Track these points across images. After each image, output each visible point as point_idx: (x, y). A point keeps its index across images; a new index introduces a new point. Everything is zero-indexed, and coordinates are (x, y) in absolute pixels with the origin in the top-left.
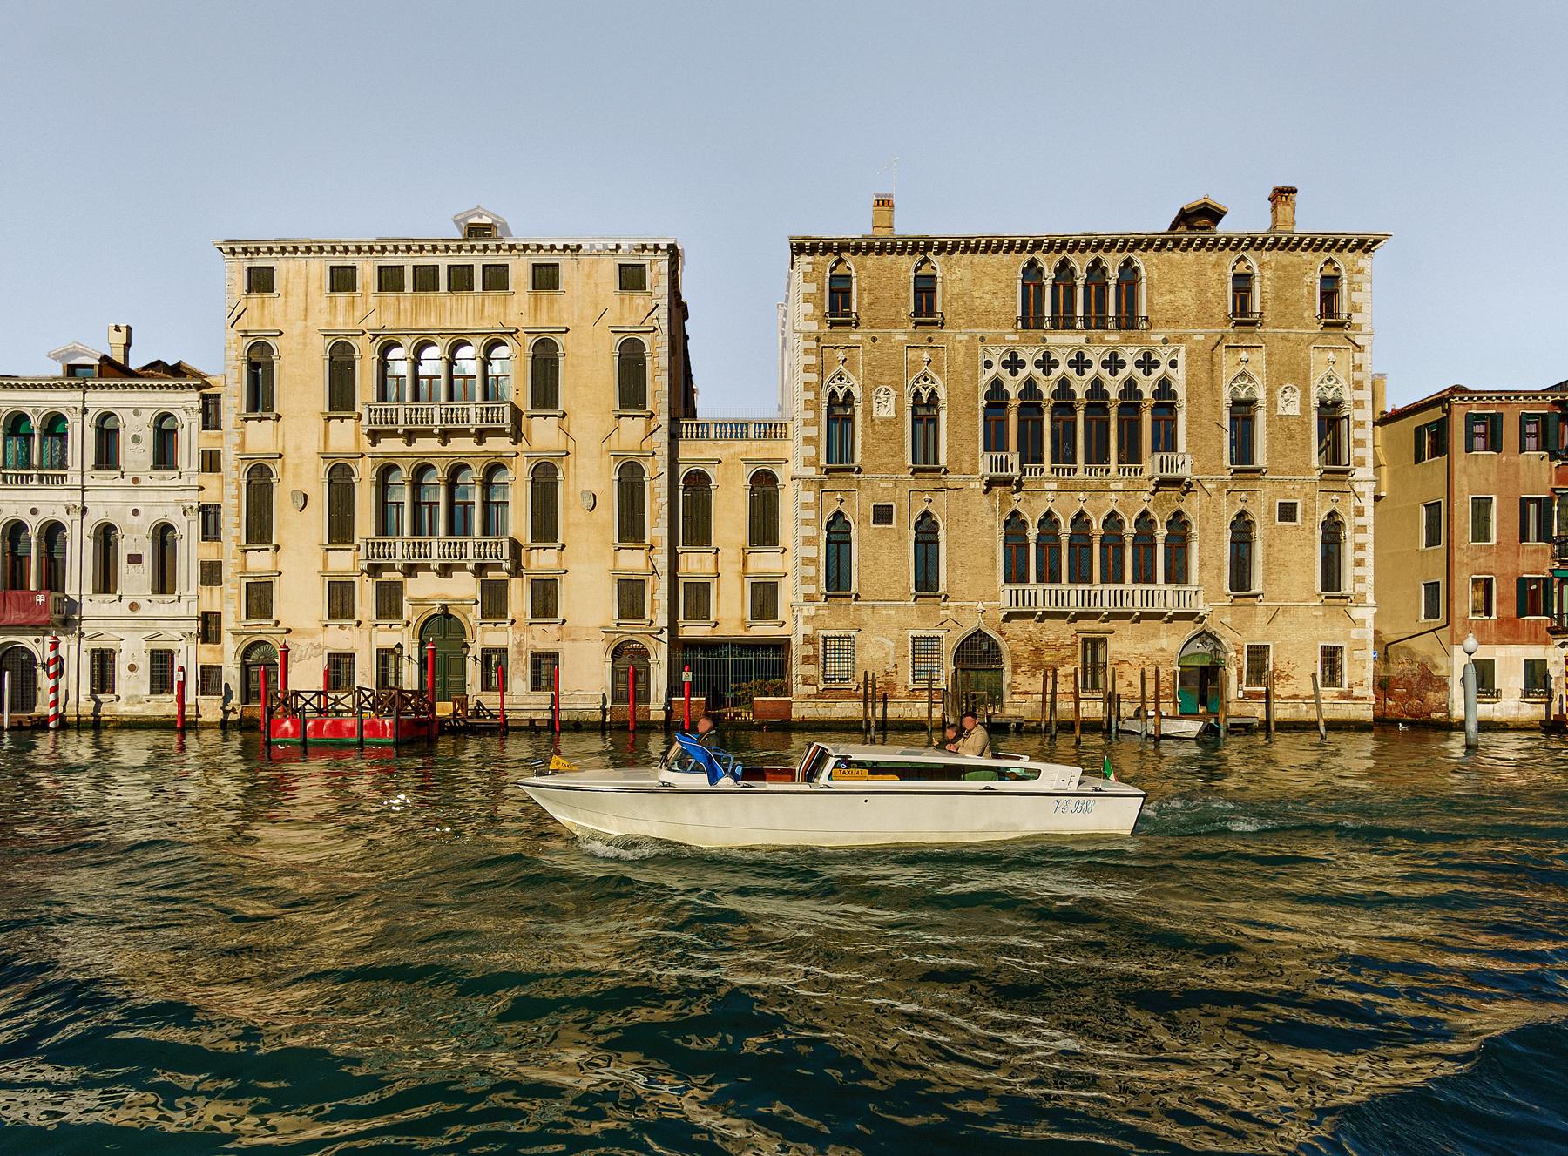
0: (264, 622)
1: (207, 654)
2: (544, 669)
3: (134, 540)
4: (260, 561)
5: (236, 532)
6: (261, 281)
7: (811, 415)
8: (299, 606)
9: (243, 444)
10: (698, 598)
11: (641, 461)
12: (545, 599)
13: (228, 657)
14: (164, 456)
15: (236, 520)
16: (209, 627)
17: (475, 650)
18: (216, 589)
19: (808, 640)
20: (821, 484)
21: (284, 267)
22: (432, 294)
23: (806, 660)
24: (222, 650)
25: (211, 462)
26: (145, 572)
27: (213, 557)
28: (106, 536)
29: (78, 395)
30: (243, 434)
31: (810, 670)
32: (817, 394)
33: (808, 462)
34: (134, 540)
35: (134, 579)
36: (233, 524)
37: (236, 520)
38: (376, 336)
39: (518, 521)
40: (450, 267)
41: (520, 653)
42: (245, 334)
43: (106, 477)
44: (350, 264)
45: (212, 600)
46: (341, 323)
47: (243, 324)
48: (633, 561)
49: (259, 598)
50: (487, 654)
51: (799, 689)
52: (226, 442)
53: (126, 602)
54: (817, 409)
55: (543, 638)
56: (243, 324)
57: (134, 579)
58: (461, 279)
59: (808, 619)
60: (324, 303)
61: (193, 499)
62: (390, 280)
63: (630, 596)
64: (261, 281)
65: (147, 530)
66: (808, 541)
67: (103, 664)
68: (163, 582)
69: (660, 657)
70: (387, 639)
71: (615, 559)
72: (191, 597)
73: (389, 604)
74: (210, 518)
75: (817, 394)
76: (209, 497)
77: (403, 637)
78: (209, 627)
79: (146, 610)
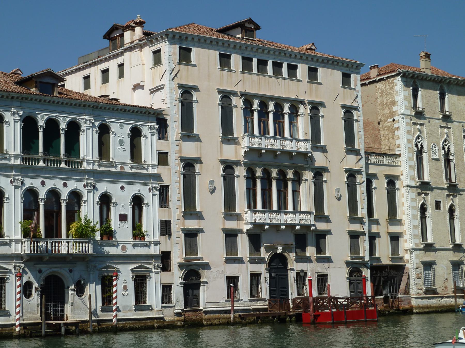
1: (165, 278)
7: (411, 155)
8: (211, 248)
9: (180, 151)
13: (176, 277)
27: (166, 217)
45: (166, 245)
54: (413, 153)
65: (129, 201)
75: (412, 145)
79: (131, 251)
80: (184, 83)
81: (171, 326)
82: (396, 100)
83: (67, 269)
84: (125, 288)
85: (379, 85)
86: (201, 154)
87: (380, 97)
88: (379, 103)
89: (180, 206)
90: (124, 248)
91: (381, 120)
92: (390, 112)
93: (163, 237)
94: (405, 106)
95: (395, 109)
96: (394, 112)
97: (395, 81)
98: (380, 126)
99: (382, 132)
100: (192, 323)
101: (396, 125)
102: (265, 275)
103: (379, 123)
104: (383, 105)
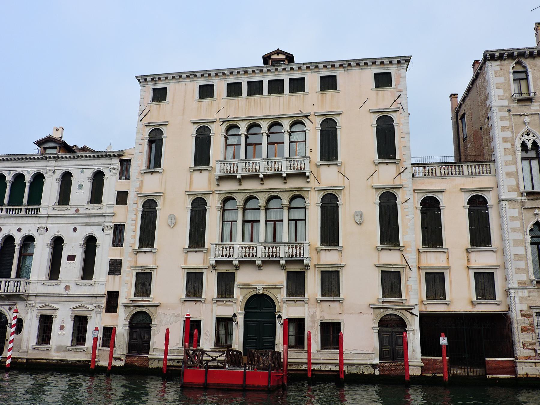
0: (146, 298)
1: (108, 320)
2: (332, 334)
4: (145, 261)
5: (132, 241)
6: (160, 95)
7: (510, 158)
8: (168, 289)
9: (141, 187)
10: (435, 283)
11: (395, 192)
12: (331, 282)
13: (120, 321)
14: (96, 197)
15: (133, 234)
18: (117, 277)
19: (523, 314)
20: (522, 203)
21: (172, 88)
22: (259, 97)
23: (525, 330)
24: (118, 316)
28: (58, 243)
29: (52, 163)
31: (527, 338)
32: (513, 145)
33: (511, 189)
34: (73, 246)
35: (71, 270)
36: (132, 236)
37: (133, 234)
38: (224, 122)
40: (269, 81)
41: (314, 322)
42: (148, 125)
43: (62, 210)
44: (210, 83)
45: (114, 284)
46: (204, 117)
47: (146, 120)
49: (144, 282)
50: (290, 321)
51: (520, 352)
52: (131, 186)
53: (63, 286)
55: (330, 312)
56: (146, 120)
58: (276, 87)
59: (522, 300)
60: (195, 105)
61: (111, 222)
62: (234, 90)
64: (160, 95)
65: (82, 241)
66: (516, 243)
67: (46, 323)
68: (88, 272)
69: (414, 326)
70: (226, 312)
71: (379, 257)
72: (103, 281)
73: (226, 285)
77: (234, 309)
78: (112, 299)
79: (74, 290)
81: (111, 371)
83: (7, 307)
84: (62, 328)
86: (165, 189)
89: (134, 244)
90: (67, 288)
93: (111, 276)
94: (498, 96)
100: (137, 373)
102: (240, 320)
103: (481, 128)
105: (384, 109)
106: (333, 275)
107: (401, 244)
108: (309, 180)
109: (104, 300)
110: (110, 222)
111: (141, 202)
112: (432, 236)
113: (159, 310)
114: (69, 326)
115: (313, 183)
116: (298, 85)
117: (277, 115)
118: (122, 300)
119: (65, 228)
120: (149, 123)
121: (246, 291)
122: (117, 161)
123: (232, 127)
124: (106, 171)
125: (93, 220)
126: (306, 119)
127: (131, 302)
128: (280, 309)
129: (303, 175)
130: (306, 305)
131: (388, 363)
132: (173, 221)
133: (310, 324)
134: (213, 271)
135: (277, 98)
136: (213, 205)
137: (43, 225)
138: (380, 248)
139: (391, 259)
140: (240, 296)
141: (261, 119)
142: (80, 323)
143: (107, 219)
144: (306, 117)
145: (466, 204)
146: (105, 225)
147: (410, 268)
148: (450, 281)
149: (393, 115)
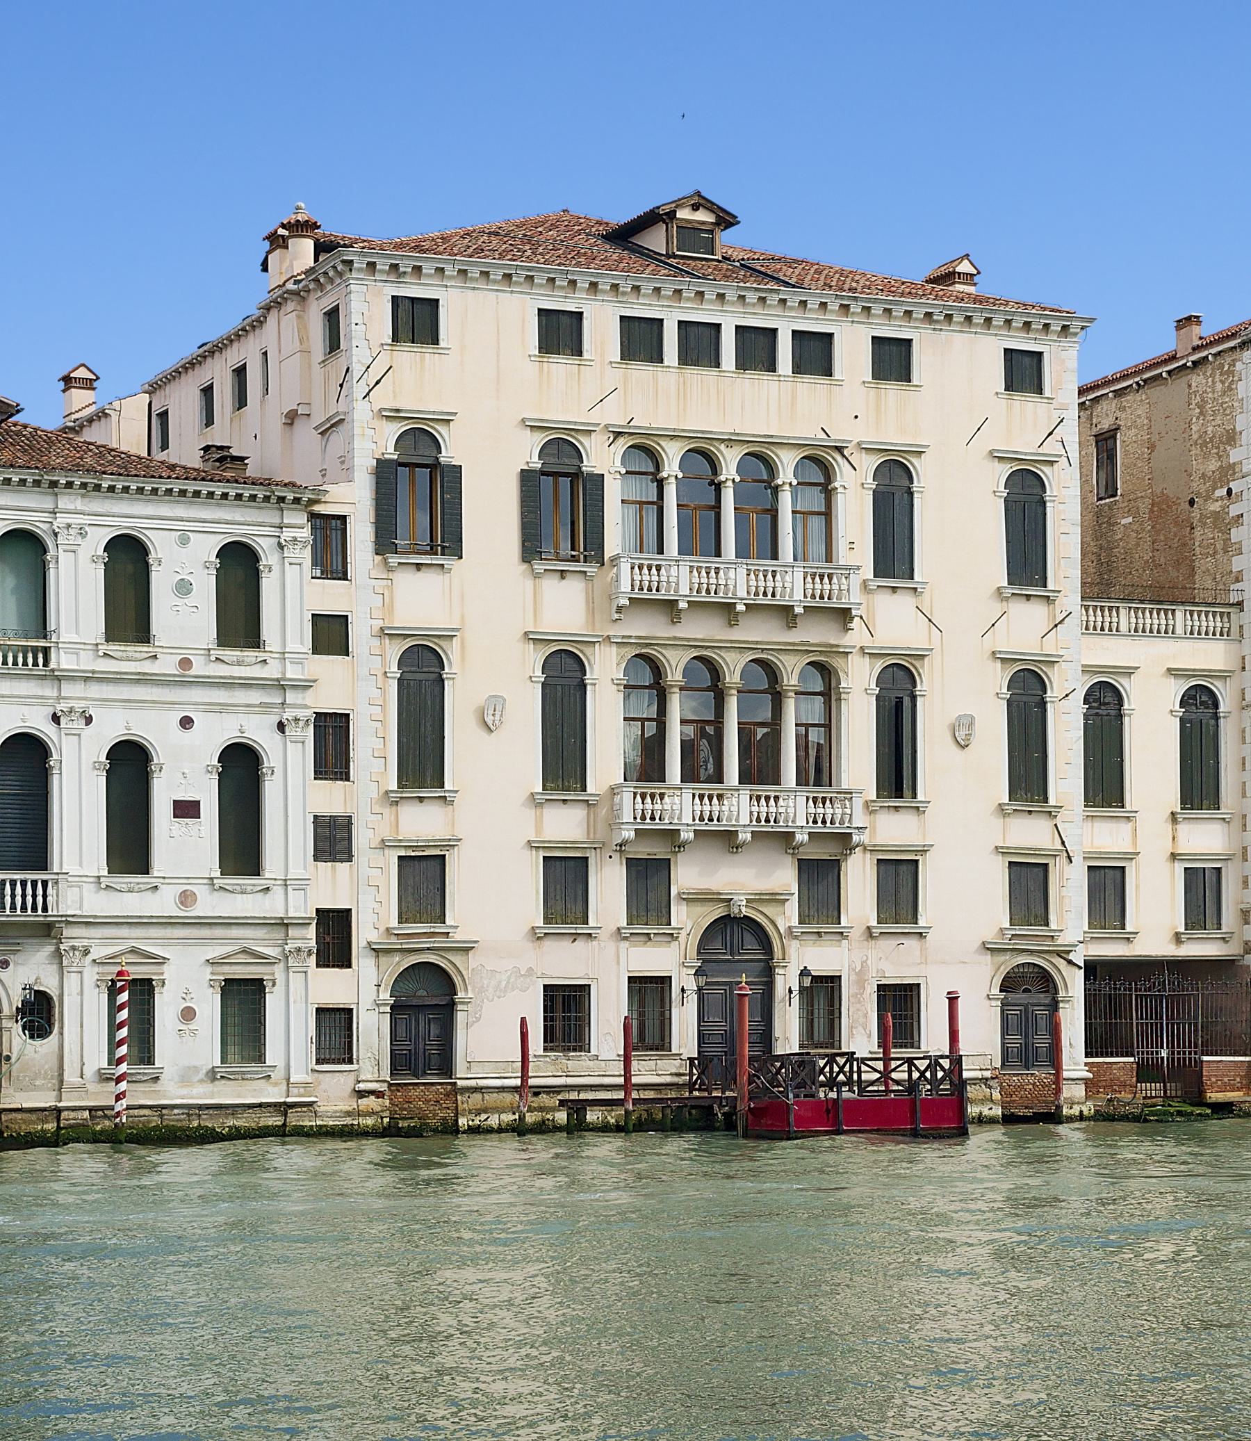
0: (440, 929)
3: (185, 772)
4: (421, 823)
10: (1108, 887)
13: (364, 987)
16: (334, 936)
17: (787, 981)
18: (343, 867)
25: (331, 634)
26: (207, 828)
30: (391, 588)
35: (186, 849)
39: (858, 759)
40: (738, 328)
42: (394, 415)
44: (571, 308)
45: (331, 886)
48: (1031, 834)
55: (895, 962)
57: (186, 849)
63: (1029, 882)
67: (135, 998)
74: (332, 744)
76: (332, 704)
79: (208, 905)
80: (409, 403)
82: (1238, 429)
84: (188, 1014)
85: (1197, 379)
86: (463, 617)
87: (1198, 418)
88: (1195, 437)
91: (1199, 495)
92: (1221, 467)
95: (1235, 455)
96: (1232, 467)
97: (1239, 365)
98: (1196, 513)
99: (1198, 533)
101: (1234, 510)
102: (685, 981)
103: (1192, 503)
104: (1205, 444)
105: (1026, 454)
106: (904, 868)
107: (1052, 801)
108: (852, 625)
109: (311, 932)
110: (306, 707)
111: (395, 651)
112: (1106, 784)
113: (474, 959)
114: (210, 1007)
115: (857, 636)
116: (815, 354)
117: (765, 436)
118: (363, 933)
119: (152, 715)
120: (398, 411)
121: (699, 909)
122: (302, 518)
123: (644, 452)
124: (265, 547)
125: (241, 696)
126: (839, 458)
127: (393, 939)
128: (784, 954)
129: (844, 616)
130: (845, 942)
131: (1016, 1077)
132: (497, 717)
133: (854, 990)
134: (616, 856)
135: (755, 384)
136: (605, 674)
137: (79, 705)
138: (1009, 809)
139: (1031, 834)
140: (688, 921)
141: (723, 440)
142: (244, 1001)
143: (291, 697)
144: (839, 449)
145: (1177, 707)
146: (288, 714)
147: (1069, 858)
148: (1137, 887)
149: (1046, 472)
